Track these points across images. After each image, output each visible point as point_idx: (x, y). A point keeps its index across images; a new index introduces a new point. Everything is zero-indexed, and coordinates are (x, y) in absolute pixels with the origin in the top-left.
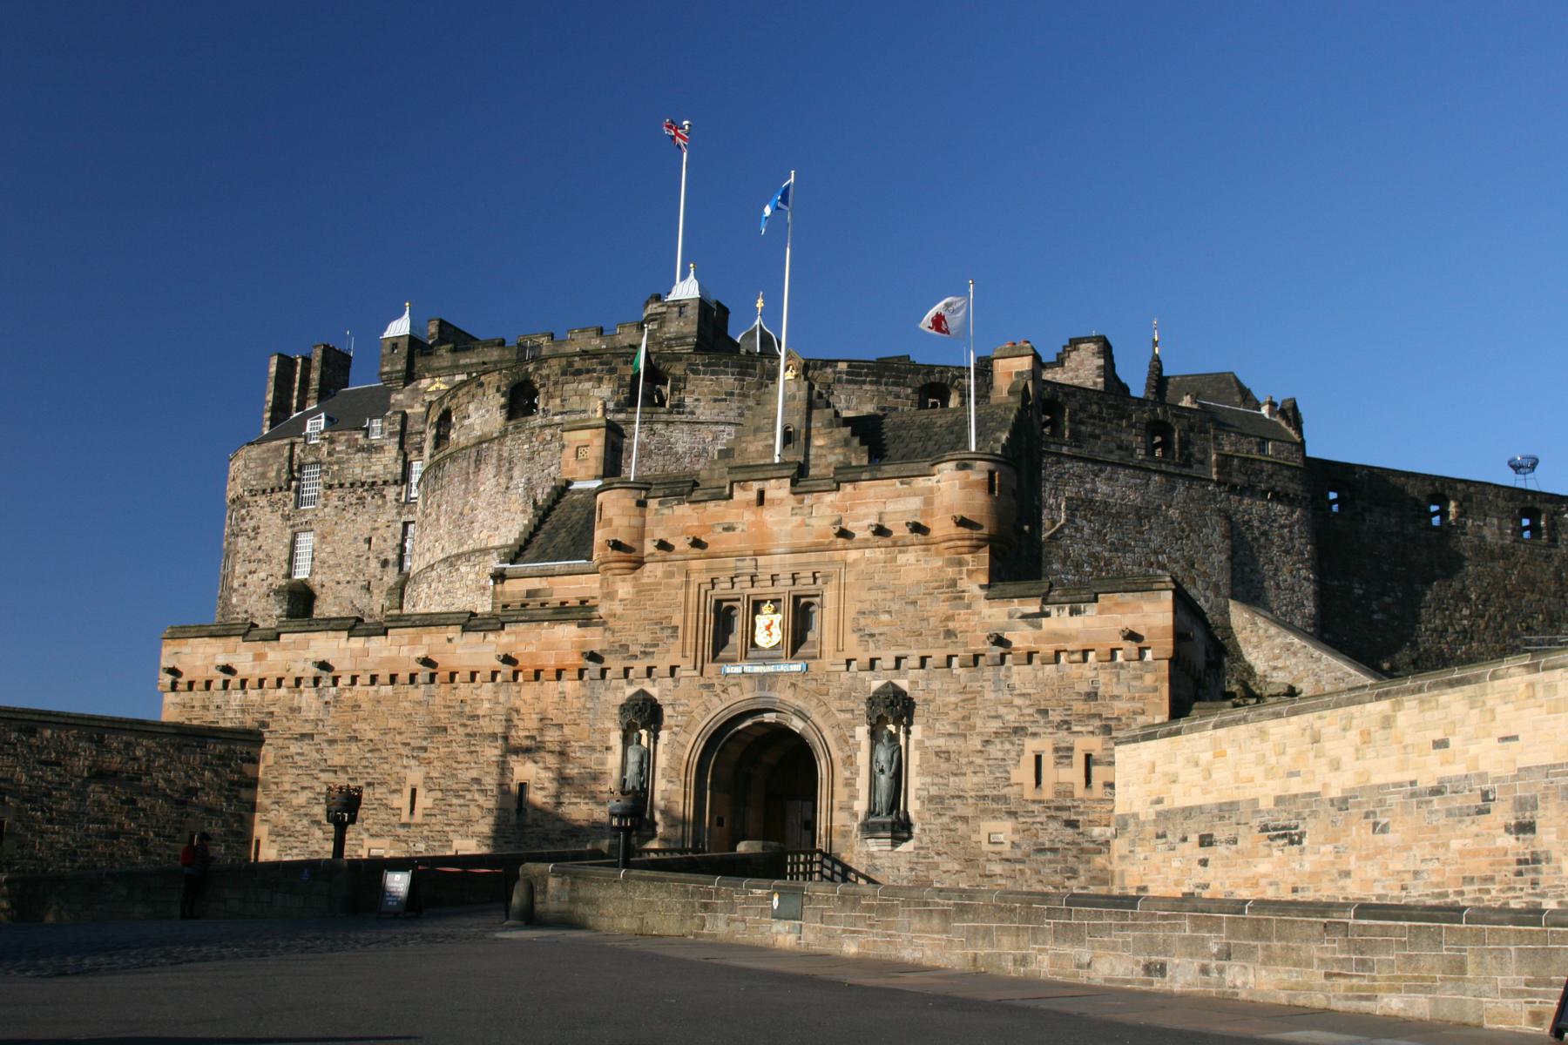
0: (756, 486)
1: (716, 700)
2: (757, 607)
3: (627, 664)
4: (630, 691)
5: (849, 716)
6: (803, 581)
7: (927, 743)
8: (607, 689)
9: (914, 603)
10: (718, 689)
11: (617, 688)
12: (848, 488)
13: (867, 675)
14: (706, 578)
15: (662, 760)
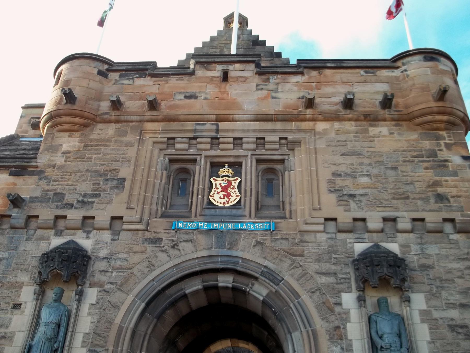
0: (220, 67)
1: (162, 256)
2: (215, 167)
3: (60, 212)
4: (56, 242)
5: (331, 280)
6: (267, 146)
7: (436, 314)
8: (28, 239)
9: (395, 168)
10: (166, 244)
11: (41, 239)
12: (314, 73)
13: (349, 238)
14: (163, 137)
15: (85, 324)
